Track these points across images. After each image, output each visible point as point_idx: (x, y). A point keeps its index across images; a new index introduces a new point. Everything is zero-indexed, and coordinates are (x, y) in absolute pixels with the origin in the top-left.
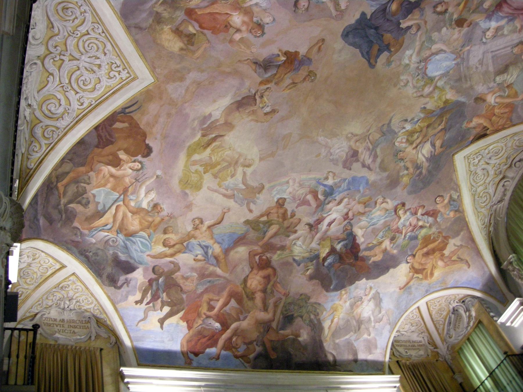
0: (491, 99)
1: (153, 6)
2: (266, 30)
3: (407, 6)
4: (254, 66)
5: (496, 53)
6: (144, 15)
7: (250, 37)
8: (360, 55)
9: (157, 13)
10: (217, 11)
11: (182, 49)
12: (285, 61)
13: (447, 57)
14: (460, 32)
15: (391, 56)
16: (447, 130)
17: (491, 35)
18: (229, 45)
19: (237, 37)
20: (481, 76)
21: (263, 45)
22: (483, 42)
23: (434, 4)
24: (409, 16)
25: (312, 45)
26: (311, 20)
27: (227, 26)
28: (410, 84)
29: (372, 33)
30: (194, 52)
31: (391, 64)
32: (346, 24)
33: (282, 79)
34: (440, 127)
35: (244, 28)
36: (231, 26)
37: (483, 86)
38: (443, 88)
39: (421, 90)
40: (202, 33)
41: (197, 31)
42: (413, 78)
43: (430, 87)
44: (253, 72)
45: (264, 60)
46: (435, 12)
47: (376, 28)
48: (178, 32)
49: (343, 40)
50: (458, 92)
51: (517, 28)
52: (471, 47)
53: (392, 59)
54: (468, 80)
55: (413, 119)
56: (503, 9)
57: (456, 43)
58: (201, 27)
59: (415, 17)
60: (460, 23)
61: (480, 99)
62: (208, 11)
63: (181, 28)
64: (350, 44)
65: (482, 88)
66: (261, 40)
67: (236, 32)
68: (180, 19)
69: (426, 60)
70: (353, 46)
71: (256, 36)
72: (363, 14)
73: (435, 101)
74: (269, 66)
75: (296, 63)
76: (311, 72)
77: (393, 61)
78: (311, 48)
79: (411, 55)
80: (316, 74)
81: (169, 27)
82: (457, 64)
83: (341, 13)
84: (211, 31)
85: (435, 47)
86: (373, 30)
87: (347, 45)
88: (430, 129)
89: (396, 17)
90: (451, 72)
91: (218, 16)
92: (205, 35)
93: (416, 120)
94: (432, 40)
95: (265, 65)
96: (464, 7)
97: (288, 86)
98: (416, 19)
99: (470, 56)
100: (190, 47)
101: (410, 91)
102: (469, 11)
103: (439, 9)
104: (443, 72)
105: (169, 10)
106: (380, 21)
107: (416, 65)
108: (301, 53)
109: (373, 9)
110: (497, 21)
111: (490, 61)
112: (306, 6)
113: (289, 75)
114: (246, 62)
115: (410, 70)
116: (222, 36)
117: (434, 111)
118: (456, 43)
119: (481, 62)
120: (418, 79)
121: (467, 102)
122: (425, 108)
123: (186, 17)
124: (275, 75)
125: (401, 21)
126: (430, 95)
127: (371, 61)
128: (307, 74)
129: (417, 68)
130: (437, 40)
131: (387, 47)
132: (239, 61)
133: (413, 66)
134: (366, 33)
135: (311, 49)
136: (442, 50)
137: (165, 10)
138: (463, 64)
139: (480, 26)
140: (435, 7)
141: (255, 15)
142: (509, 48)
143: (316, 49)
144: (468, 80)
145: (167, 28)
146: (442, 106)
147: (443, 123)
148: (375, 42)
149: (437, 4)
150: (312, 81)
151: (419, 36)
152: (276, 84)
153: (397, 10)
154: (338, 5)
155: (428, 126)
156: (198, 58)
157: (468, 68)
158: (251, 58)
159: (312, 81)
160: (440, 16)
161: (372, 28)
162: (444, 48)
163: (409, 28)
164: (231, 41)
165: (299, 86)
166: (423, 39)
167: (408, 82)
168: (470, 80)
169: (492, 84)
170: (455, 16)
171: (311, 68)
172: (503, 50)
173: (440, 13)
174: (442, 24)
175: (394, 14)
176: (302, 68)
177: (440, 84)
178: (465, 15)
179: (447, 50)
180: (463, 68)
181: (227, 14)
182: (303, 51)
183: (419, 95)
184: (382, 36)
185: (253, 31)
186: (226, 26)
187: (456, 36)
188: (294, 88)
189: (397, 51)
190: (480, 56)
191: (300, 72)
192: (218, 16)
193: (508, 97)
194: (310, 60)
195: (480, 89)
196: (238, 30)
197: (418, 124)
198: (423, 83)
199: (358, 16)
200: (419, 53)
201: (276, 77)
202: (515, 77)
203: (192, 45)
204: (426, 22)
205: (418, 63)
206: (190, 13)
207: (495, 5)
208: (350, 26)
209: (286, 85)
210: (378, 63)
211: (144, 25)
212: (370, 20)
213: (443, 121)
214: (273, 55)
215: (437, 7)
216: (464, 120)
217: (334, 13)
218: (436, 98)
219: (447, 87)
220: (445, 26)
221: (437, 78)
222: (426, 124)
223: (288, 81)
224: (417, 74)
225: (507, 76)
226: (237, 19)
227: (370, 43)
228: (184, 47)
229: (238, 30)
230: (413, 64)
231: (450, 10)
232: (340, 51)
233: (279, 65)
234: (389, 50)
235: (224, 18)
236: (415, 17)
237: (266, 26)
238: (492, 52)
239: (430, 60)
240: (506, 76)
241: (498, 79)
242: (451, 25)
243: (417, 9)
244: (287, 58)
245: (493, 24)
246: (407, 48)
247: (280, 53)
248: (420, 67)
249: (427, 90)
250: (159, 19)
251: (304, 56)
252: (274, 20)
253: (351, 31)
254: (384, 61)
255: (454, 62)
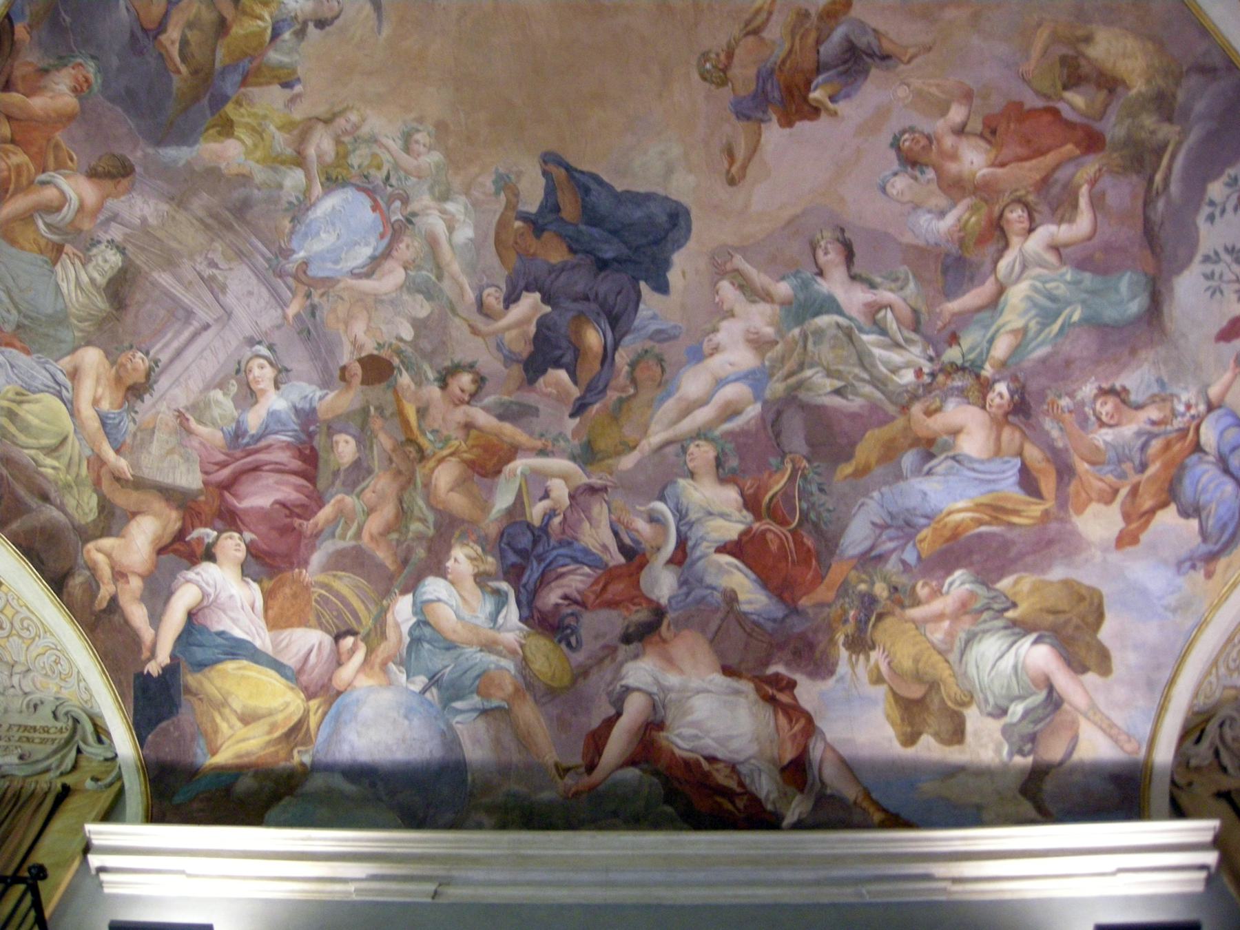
0: (75, 189)
1: (1184, 134)
2: (892, 154)
3: (558, 353)
4: (887, 47)
5: (191, 329)
6: (1200, 106)
7: (925, 125)
8: (606, 179)
9: (1169, 120)
10: (1027, 164)
11: (1088, 39)
12: (808, 90)
13: (336, 262)
14: (354, 343)
15: (510, 206)
16: (139, 34)
17: (256, 372)
18: (969, 83)
19: (957, 114)
20: (174, 244)
21: (882, 114)
22: (259, 343)
23: (489, 385)
24: (532, 329)
25: (756, 158)
26: (790, 222)
27: (990, 133)
28: (395, 146)
29: (605, 247)
30: (1055, 38)
31: (495, 182)
32: (691, 244)
33: (793, 33)
34: (173, 34)
35: (949, 141)
36: (982, 136)
37: (144, 220)
38: (275, 170)
39: (346, 139)
40: (1047, 97)
41: (1061, 99)
42: (397, 166)
43: (319, 157)
44: (882, 28)
45: (865, 72)
46: (471, 367)
47: (603, 265)
48: (1110, 84)
49: (676, 202)
50: (212, 175)
51: (200, 422)
52: (285, 317)
53: (503, 197)
54: (210, 221)
55: (301, 34)
56: (288, 453)
57: (341, 310)
58: (1055, 112)
59: (514, 333)
60: (377, 369)
61: (114, 172)
62: (1050, 159)
63: (1102, 95)
64: (649, 197)
65: (139, 213)
66: (895, 124)
67: (964, 125)
68: (1112, 117)
69: (395, 232)
70: (638, 193)
71: (912, 130)
72: (662, 287)
73: (265, 117)
74: (845, 62)
75: (776, 94)
76: (723, 82)
77: (497, 193)
78: (755, 150)
79: (451, 229)
80: (704, 78)
81: (1133, 92)
82: (286, 253)
83: (720, 267)
84: (1027, 106)
85: (392, 278)
86: (609, 255)
87: (660, 191)
88: (208, 16)
89: (570, 315)
90: (287, 224)
91: (1021, 151)
92: (1038, 93)
93: (287, 35)
94: (419, 291)
95: (857, 61)
96: (400, 413)
97: (768, 19)
98: (509, 328)
99: (264, 290)
100: (1064, 50)
101: (381, 124)
102: (380, 409)
103: (466, 380)
104: (312, 215)
105: (1143, 135)
106: (606, 285)
107: (414, 206)
108: (774, 124)
109: (644, 311)
110: (272, 414)
111: (187, 299)
112: (820, 253)
113: (780, 53)
114: (911, 51)
115: (425, 187)
116: (997, 103)
117: (244, 83)
118: (341, 310)
119: (215, 287)
120: (379, 168)
121: (150, 151)
122: (287, 85)
123: (1098, 126)
124: (819, 42)
125: (548, 309)
126: (303, 131)
127: (562, 171)
128: (730, 74)
129: (405, 201)
130: (406, 297)
131: (536, 225)
132: (930, 49)
133: (423, 200)
134: (625, 243)
135: (754, 148)
136: (368, 275)
137: (1153, 132)
138: (268, 260)
139: (310, 382)
140: (480, 381)
141: (934, 187)
142: (164, 358)
143: (740, 154)
144: (210, 221)
145: (1138, 86)
146: (229, 109)
147: (175, 51)
148: (583, 227)
149: (479, 389)
150: (705, 56)
151: (467, 287)
152: (804, 15)
153: (578, 333)
154: (741, 287)
155: (222, 26)
156: (1039, 25)
157: (240, 255)
158: (902, 67)
159: (705, 56)
160: (448, 363)
161: (615, 259)
162: (367, 285)
163: (511, 299)
164: (967, 96)
165: (736, 31)
166: (446, 285)
167: (407, 149)
168: (201, 221)
169: (116, 232)
170: (405, 379)
171: (726, 92)
172: (176, 344)
173: (455, 370)
174: (426, 345)
175: (580, 318)
176: (753, 87)
177: (294, 179)
178: (378, 393)
179: (349, 281)
180: (256, 248)
181: (1003, 165)
182: (773, 134)
183: (341, 122)
184: (571, 250)
185: (923, 142)
186: (994, 132)
187: (359, 328)
188: (747, 16)
189: (502, 225)
190: (229, 300)
191: (752, 72)
192: (1021, 151)
193: (27, 218)
194: (742, 114)
195: (141, 207)
196: (960, 131)
197: (266, 24)
198: (354, 160)
199: (674, 276)
200: (432, 243)
201: (813, 36)
202: (64, 286)
203: (1064, 60)
204: (475, 331)
205: (414, 214)
206: (1092, 142)
207: (322, 454)
208: (679, 245)
209: (774, 17)
210: (540, 172)
211: (1194, 81)
212: (635, 280)
213: (184, 59)
214: (848, 96)
215: (474, 381)
216: (106, 85)
217: (739, 262)
218: (272, 128)
219: (260, 174)
220: (414, 343)
221: (318, 189)
222: (237, 30)
223: (775, 31)
224: (393, 181)
225: (92, 280)
226: (974, 159)
227: (592, 217)
228: (1082, 47)
229: (960, 131)
230: (427, 208)
231: (434, 391)
232: (669, 170)
233: (819, 70)
234: (524, 217)
235: (1007, 153)
236: (514, 333)
237: (896, 166)
238: (207, 327)
239: (382, 236)
240: (96, 275)
241: (115, 259)
242: (399, 352)
243: (525, 355)
244: (805, 99)
245: (275, 402)
246: (476, 244)
247: (831, 106)
248: (398, 204)
249: (322, 144)
250: (1163, 104)
251: (762, 121)
252: (883, 190)
253: (667, 232)
254: (523, 186)
255: (302, 254)
